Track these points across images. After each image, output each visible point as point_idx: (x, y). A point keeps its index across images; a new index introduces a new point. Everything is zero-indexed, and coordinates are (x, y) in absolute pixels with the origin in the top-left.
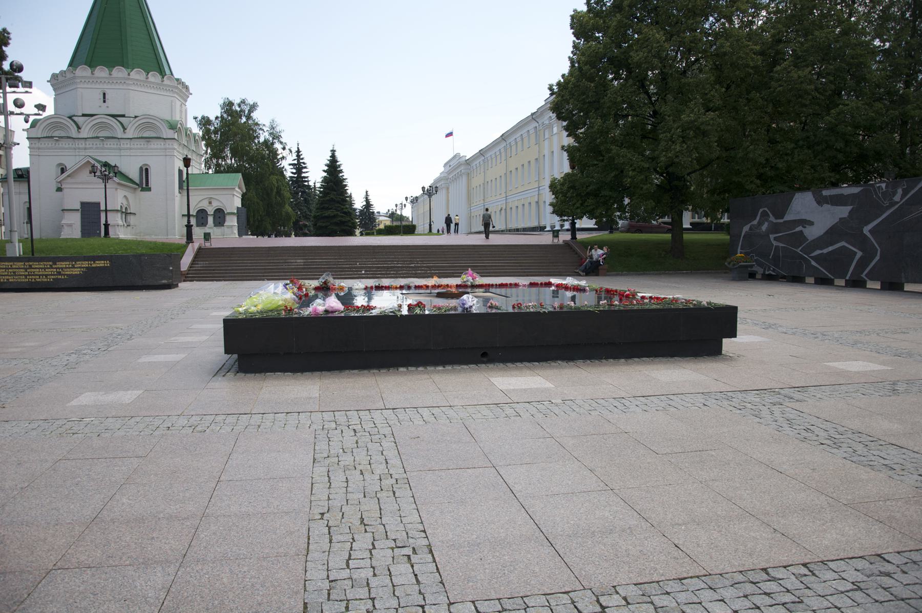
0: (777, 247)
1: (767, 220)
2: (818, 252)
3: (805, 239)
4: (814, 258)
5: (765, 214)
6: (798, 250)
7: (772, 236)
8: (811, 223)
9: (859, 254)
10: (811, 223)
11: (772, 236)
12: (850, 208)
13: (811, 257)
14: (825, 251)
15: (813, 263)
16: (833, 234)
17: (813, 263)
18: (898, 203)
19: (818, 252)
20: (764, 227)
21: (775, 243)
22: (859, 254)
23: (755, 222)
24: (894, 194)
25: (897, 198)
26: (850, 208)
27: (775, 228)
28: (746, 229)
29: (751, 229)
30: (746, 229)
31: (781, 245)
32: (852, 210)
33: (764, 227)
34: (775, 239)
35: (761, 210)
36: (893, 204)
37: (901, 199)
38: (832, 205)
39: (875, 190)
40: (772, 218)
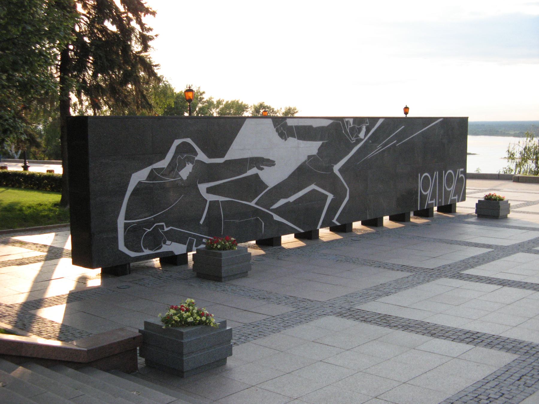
0: (213, 204)
1: (191, 160)
2: (282, 202)
3: (263, 186)
4: (276, 211)
5: (184, 149)
6: (253, 204)
7: (203, 188)
8: (270, 163)
9: (330, 197)
10: (270, 163)
11: (203, 188)
12: (320, 143)
13: (272, 210)
14: (292, 199)
15: (276, 218)
16: (302, 175)
17: (276, 218)
18: (362, 140)
19: (282, 202)
20: (185, 172)
21: (211, 198)
22: (330, 197)
23: (163, 164)
24: (360, 130)
25: (362, 135)
26: (320, 143)
27: (207, 173)
28: (140, 176)
29: (151, 176)
30: (140, 176)
31: (221, 199)
32: (322, 146)
33: (185, 172)
34: (210, 190)
35: (177, 142)
36: (359, 141)
37: (365, 136)
38: (299, 138)
39: (344, 125)
40: (201, 156)
